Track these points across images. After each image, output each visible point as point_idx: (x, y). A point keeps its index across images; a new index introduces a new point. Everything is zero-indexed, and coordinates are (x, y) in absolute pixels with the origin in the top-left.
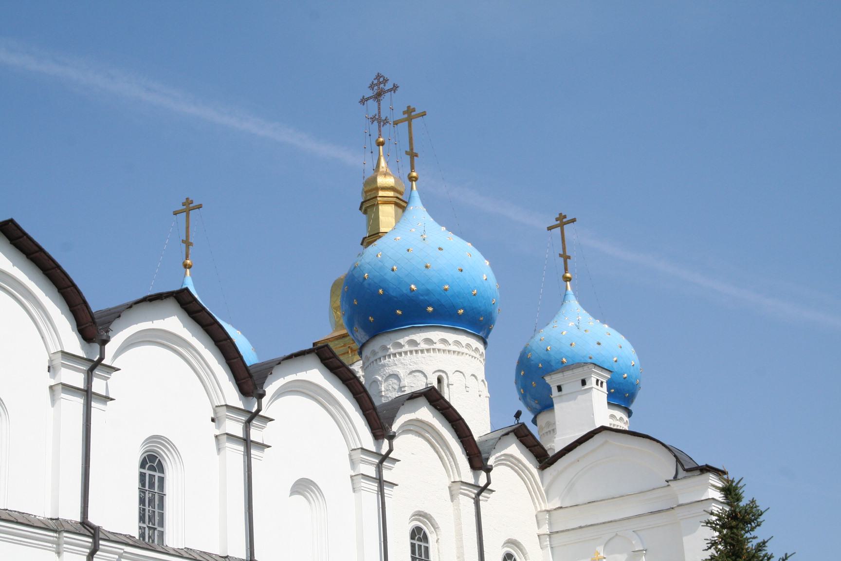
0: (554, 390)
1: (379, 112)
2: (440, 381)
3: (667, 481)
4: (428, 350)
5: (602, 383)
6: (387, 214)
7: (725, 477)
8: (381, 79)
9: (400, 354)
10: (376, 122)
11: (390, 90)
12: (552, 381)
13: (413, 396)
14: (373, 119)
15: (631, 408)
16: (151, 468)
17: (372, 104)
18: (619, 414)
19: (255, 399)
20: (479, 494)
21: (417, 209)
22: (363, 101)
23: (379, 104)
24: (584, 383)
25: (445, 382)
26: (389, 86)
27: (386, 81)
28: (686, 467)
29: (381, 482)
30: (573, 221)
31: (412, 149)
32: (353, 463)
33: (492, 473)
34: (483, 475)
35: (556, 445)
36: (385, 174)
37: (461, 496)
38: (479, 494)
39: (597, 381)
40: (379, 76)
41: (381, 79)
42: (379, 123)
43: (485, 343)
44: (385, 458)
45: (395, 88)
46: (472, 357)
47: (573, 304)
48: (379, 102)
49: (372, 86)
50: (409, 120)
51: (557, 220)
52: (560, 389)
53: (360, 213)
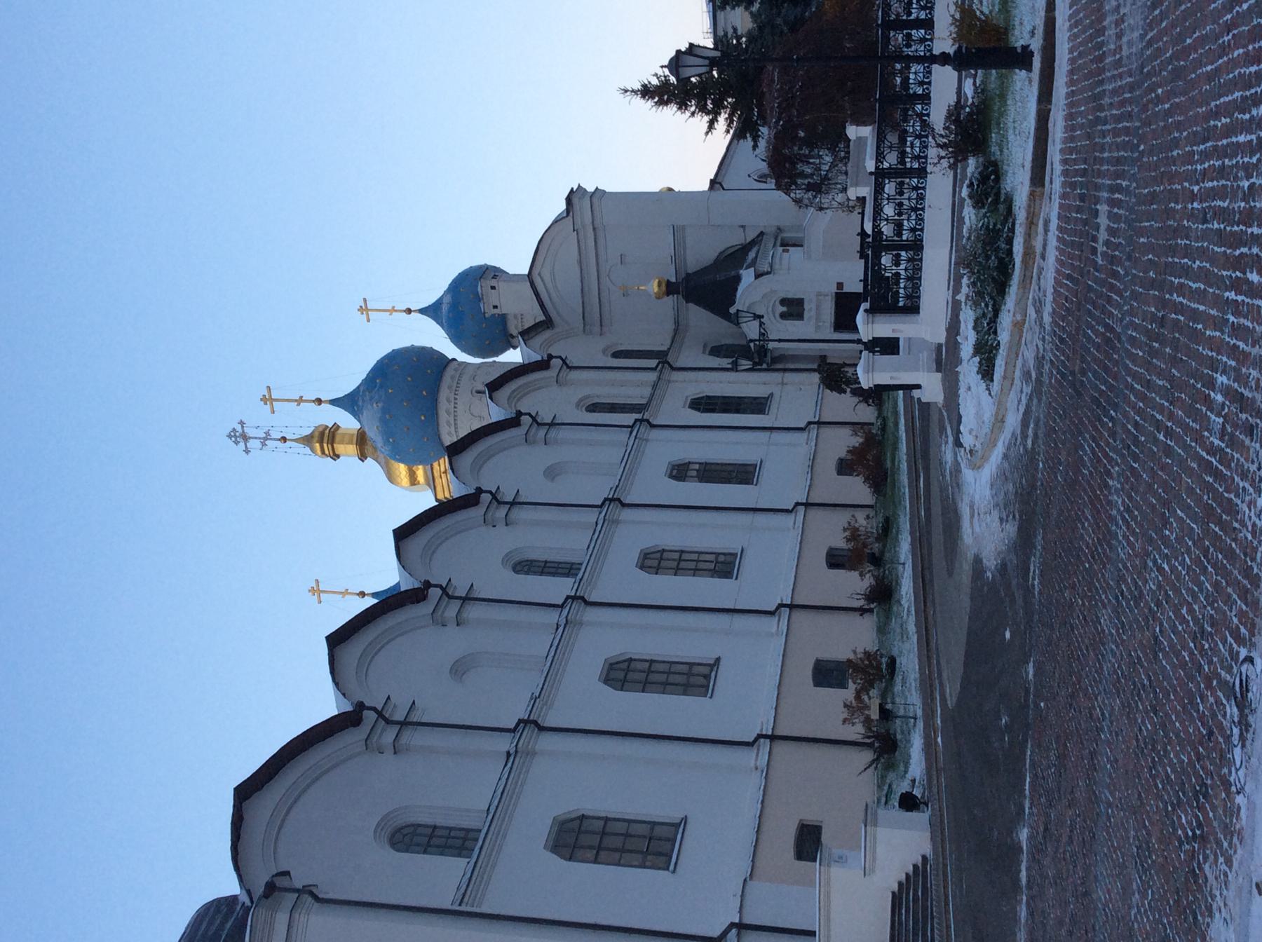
1: (260, 438)
3: (574, 230)
8: (232, 434)
10: (267, 442)
11: (243, 427)
12: (490, 312)
14: (264, 444)
17: (251, 444)
19: (483, 495)
20: (568, 367)
22: (247, 451)
23: (252, 438)
24: (493, 288)
26: (239, 428)
27: (234, 430)
28: (565, 215)
29: (552, 424)
30: (365, 300)
31: (296, 401)
32: (534, 442)
33: (554, 355)
34: (554, 361)
35: (536, 315)
37: (568, 377)
38: (568, 367)
40: (230, 436)
41: (232, 434)
42: (267, 439)
44: (534, 419)
45: (242, 423)
46: (456, 403)
48: (250, 438)
49: (237, 443)
50: (272, 400)
51: (363, 314)
52: (495, 307)
53: (338, 460)
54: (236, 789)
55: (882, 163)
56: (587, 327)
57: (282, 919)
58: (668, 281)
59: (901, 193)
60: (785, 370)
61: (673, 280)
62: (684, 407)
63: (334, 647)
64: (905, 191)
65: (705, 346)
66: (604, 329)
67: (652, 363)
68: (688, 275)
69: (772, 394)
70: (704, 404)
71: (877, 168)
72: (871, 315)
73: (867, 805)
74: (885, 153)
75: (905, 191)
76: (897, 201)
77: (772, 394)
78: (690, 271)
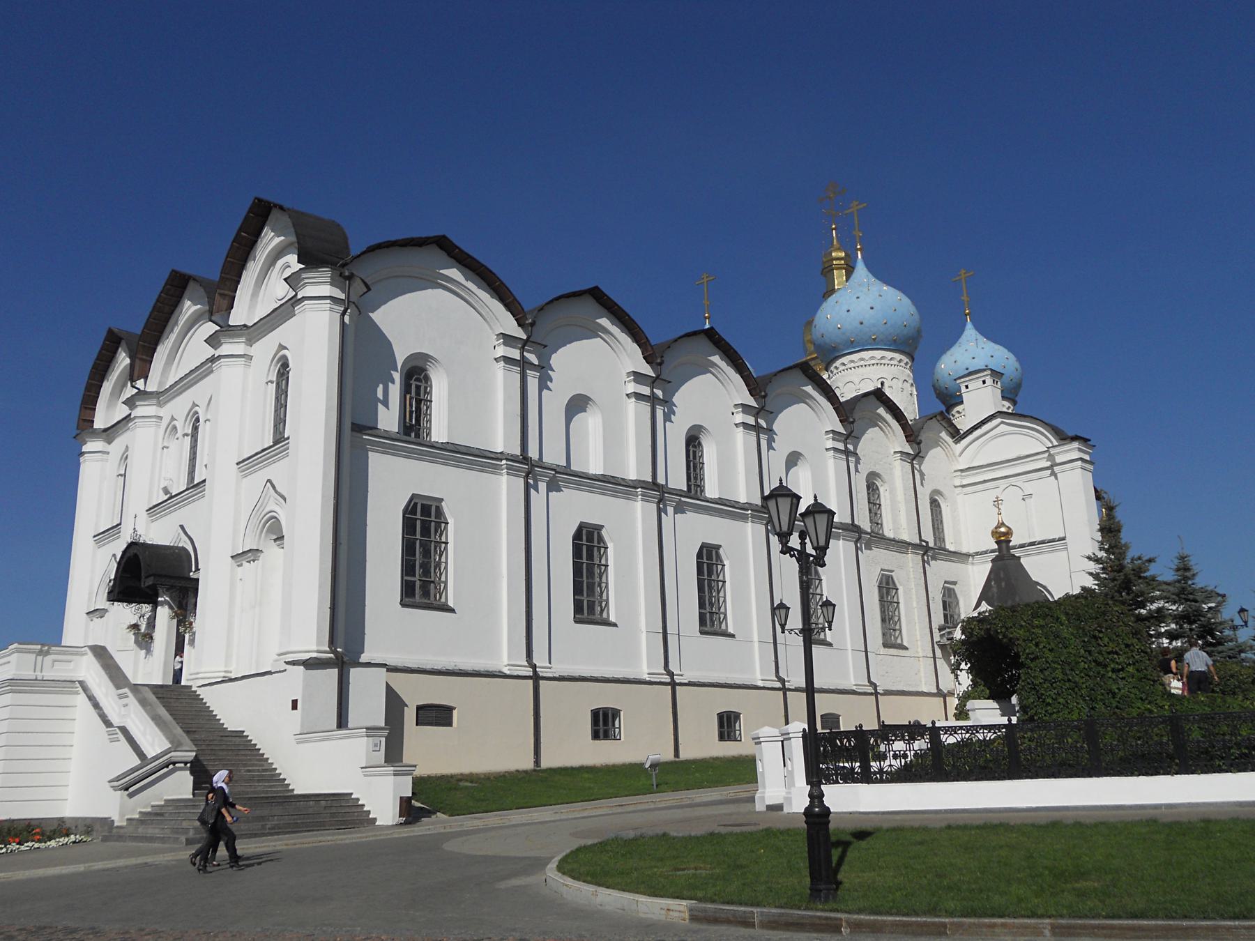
0: (963, 389)
2: (882, 384)
3: (1047, 448)
4: (873, 365)
5: (997, 382)
6: (839, 277)
7: (1089, 443)
9: (854, 368)
13: (866, 395)
15: (1017, 399)
16: (694, 446)
18: (1007, 404)
21: (861, 270)
25: (886, 385)
33: (921, 445)
35: (963, 424)
36: (839, 249)
39: (994, 381)
43: (913, 359)
47: (970, 331)
52: (967, 387)
54: (444, 236)
55: (946, 733)
56: (959, 473)
57: (326, 290)
58: (1011, 541)
59: (895, 757)
60: (934, 658)
61: (1011, 544)
62: (882, 570)
63: (590, 294)
64: (898, 761)
65: (955, 583)
66: (960, 488)
67: (928, 536)
68: (1019, 557)
69: (906, 648)
70: (887, 586)
71: (940, 728)
72: (800, 735)
73: (415, 766)
74: (955, 735)
75: (898, 761)
76: (908, 752)
77: (906, 648)
78: (1022, 561)
